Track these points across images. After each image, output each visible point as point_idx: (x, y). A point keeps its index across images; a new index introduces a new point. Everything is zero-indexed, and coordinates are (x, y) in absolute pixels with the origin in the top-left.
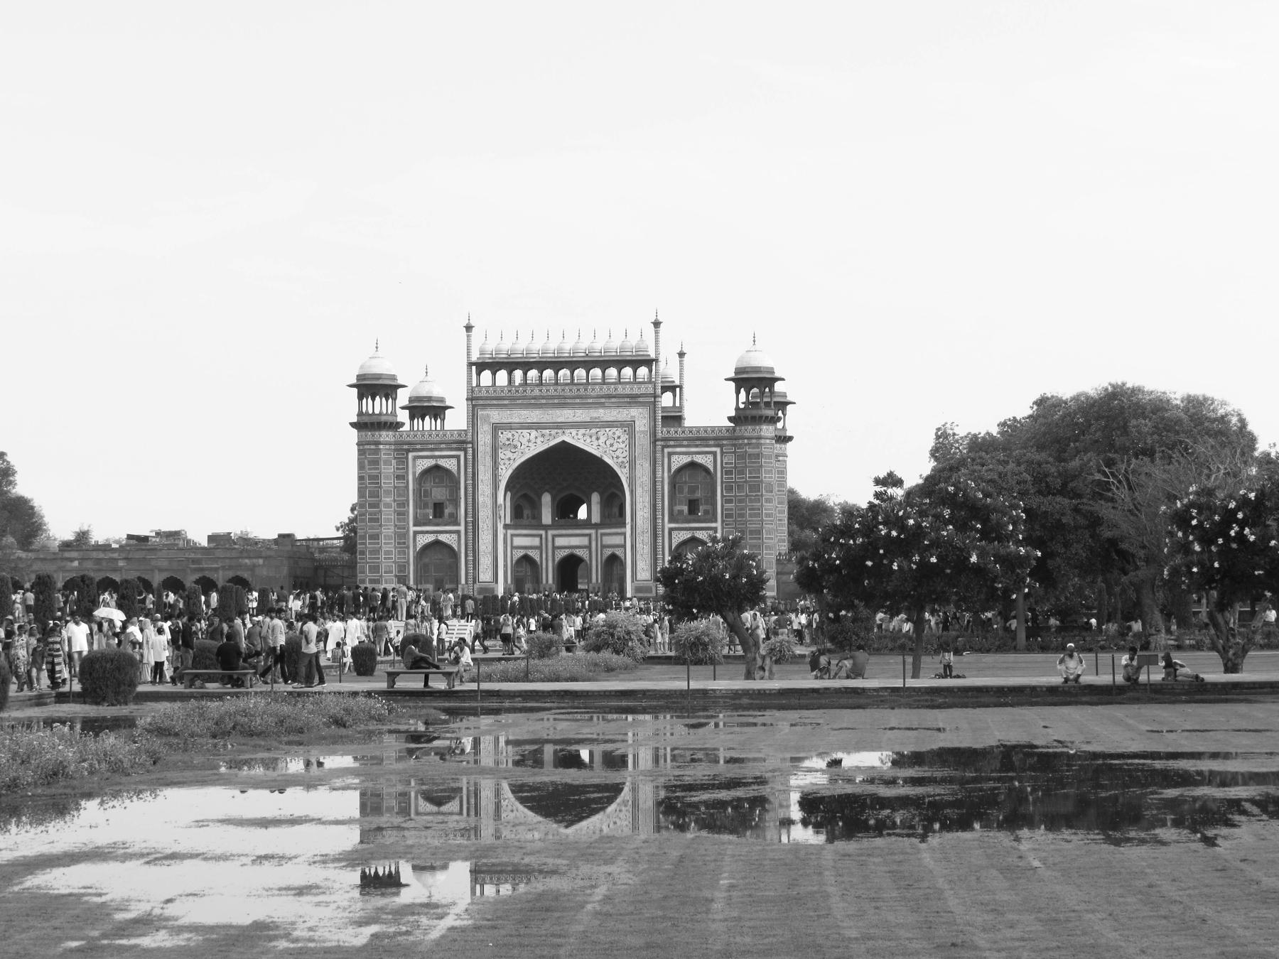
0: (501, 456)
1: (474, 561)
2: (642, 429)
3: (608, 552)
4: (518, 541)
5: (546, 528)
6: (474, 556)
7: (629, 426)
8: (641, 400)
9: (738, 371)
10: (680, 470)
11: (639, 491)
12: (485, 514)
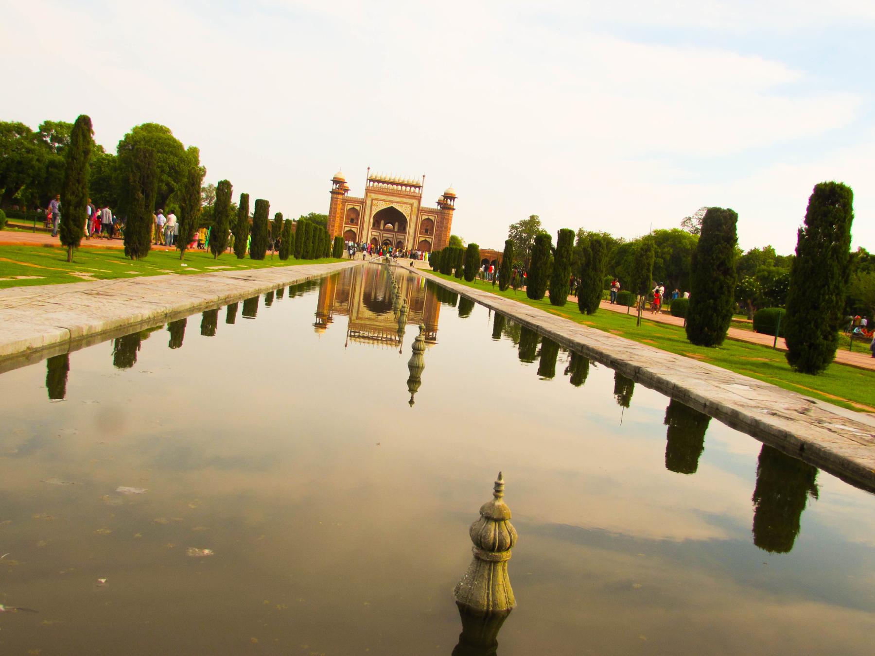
7: (412, 205)
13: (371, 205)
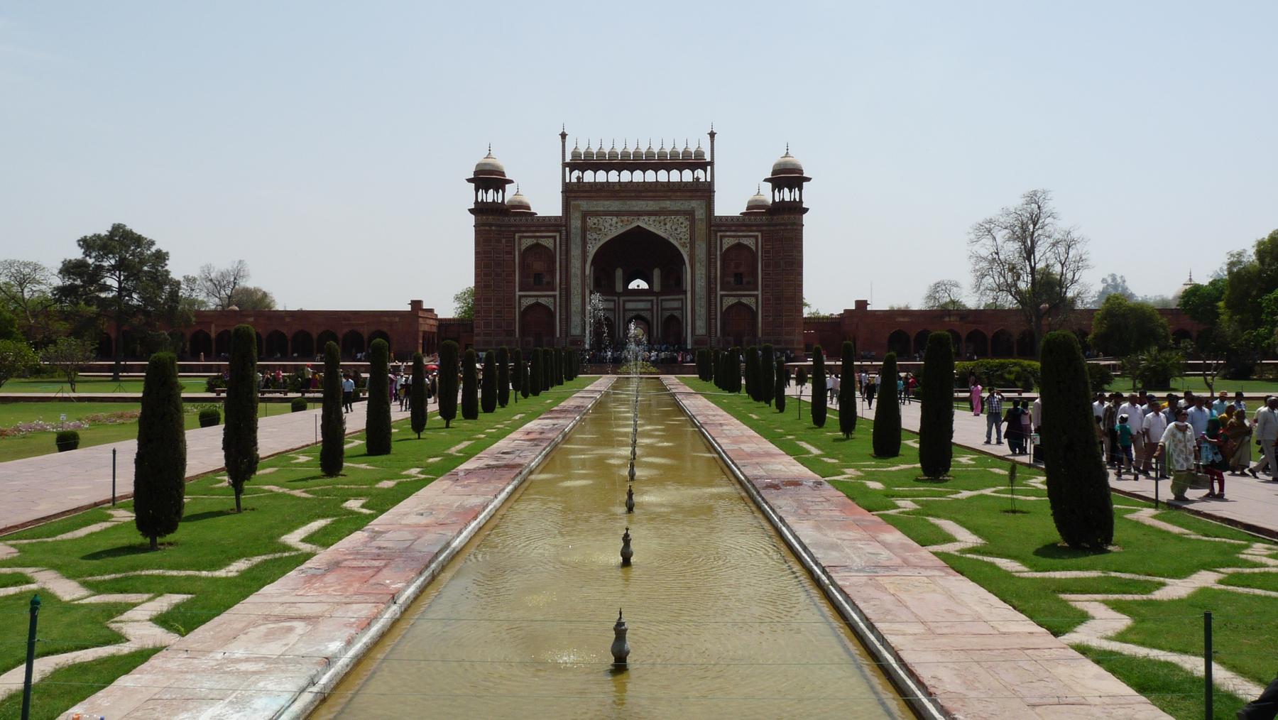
3: (668, 314)
5: (619, 295)
7: (690, 214)
9: (774, 173)
10: (728, 250)
11: (698, 265)
12: (576, 283)
13: (584, 230)
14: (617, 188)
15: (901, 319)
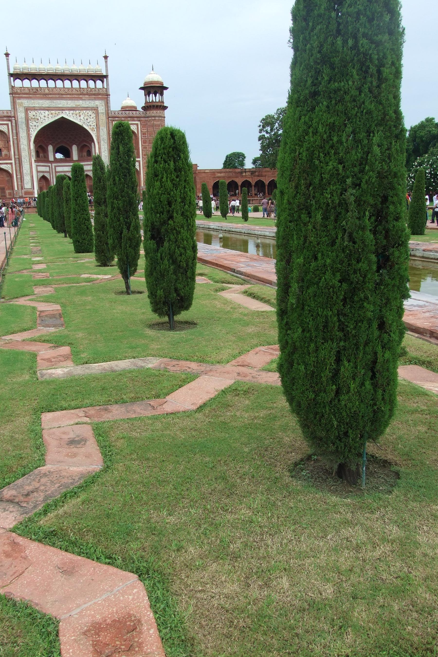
0: (30, 124)
1: (21, 178)
2: (102, 111)
4: (41, 169)
5: (51, 162)
6: (21, 176)
7: (95, 109)
8: (100, 96)
11: (102, 143)
12: (25, 154)
13: (27, 120)
14: (47, 91)
15: (219, 175)
